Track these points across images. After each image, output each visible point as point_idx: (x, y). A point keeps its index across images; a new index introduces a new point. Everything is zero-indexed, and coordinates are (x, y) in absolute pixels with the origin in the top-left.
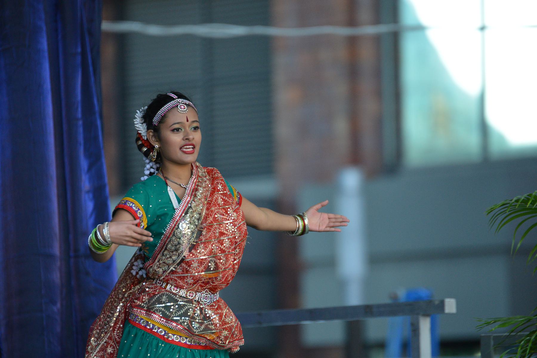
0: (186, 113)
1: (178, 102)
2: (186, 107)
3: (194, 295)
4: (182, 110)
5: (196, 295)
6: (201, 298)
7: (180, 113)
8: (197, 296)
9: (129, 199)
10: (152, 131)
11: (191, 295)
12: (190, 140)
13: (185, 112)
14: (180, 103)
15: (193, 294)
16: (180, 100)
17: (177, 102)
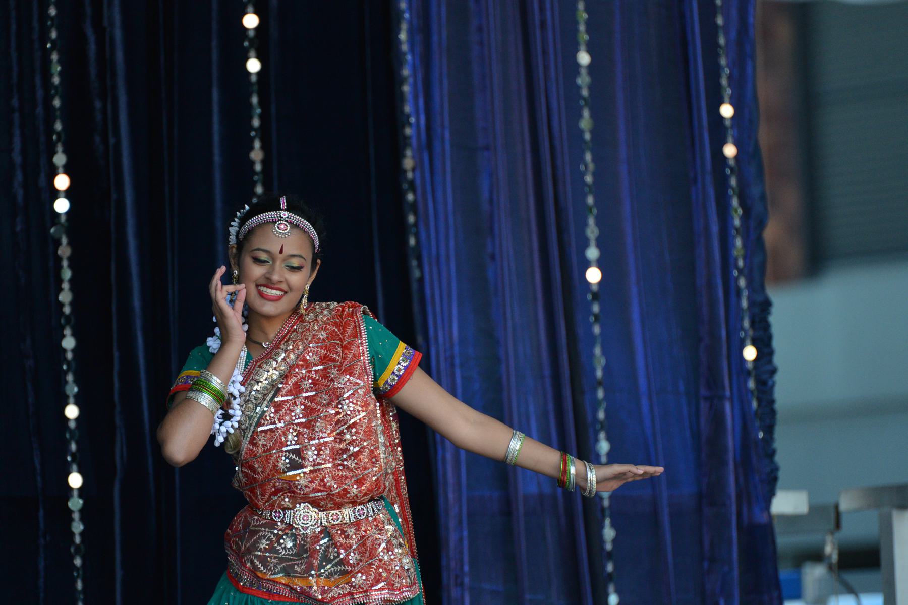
2: (289, 228)
5: (284, 515)
6: (293, 519)
9: (191, 373)
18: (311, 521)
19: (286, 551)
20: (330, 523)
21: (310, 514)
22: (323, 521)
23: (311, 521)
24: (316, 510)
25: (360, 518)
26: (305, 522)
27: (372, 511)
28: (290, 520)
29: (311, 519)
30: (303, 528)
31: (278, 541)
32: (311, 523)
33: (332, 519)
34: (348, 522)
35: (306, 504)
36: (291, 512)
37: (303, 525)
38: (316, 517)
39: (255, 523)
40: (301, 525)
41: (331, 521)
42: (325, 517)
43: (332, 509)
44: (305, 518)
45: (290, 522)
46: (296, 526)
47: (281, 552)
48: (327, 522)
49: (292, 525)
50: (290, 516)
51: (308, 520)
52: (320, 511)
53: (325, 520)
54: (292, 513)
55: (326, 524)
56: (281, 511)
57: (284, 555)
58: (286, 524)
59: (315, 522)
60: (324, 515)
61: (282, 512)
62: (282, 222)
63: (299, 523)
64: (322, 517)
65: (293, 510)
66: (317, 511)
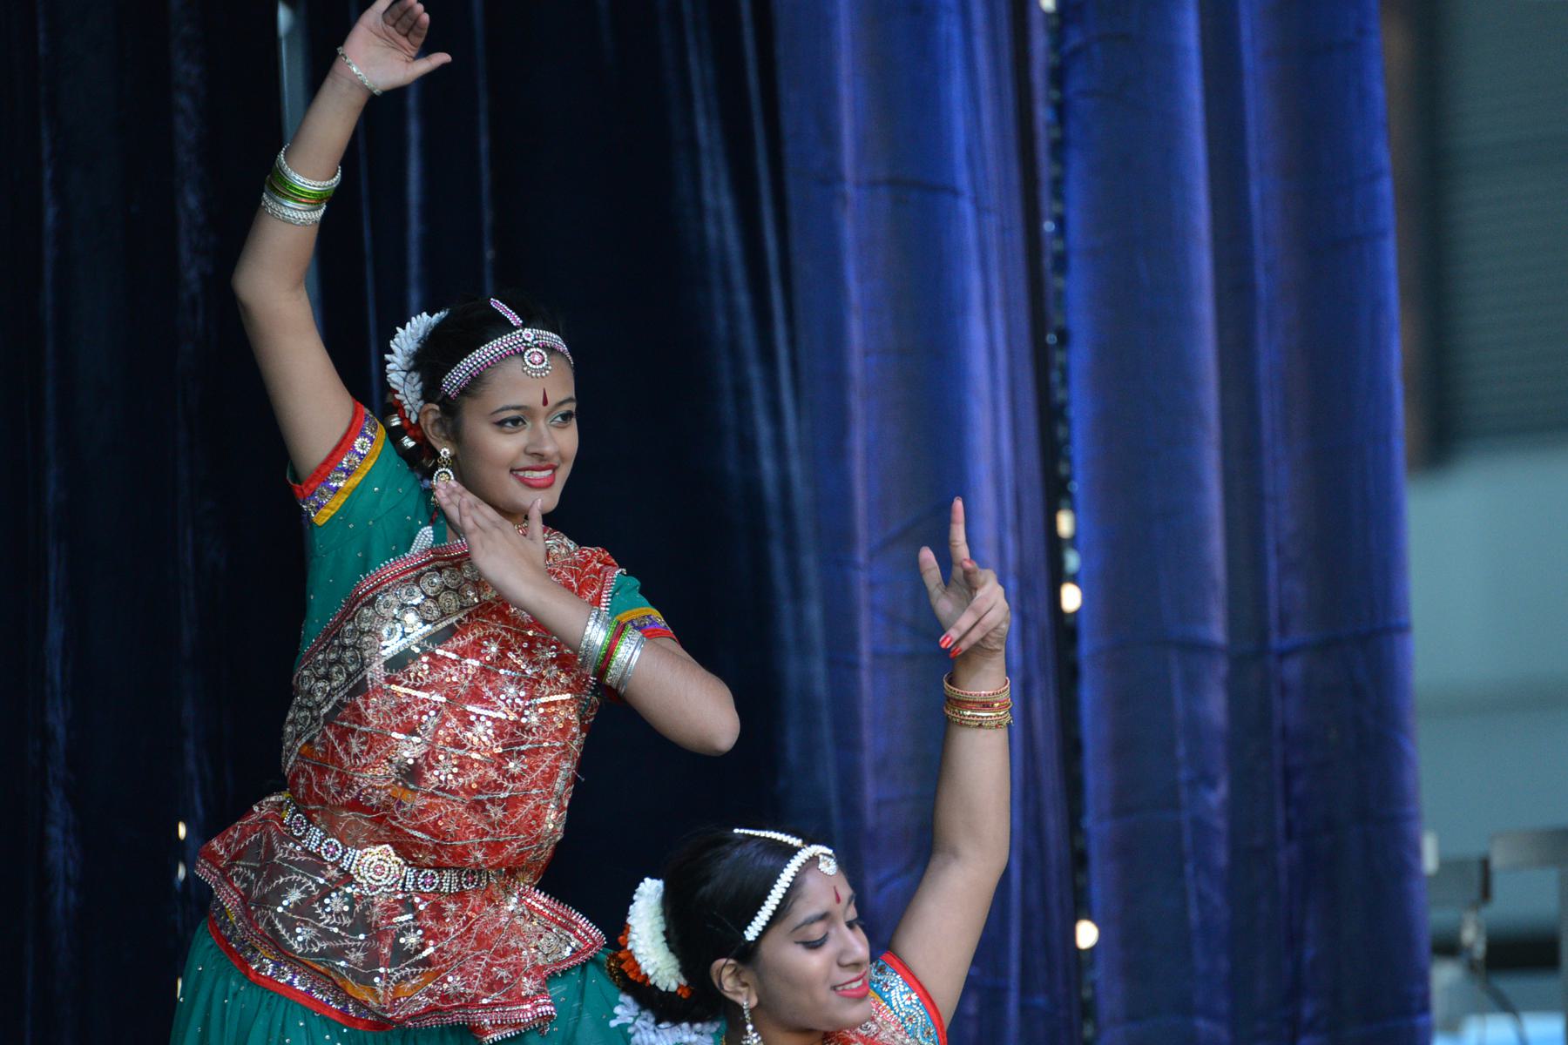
0: (541, 376)
1: (525, 341)
3: (339, 854)
4: (534, 367)
5: (343, 854)
7: (532, 377)
8: (348, 858)
10: (437, 408)
11: (429, 880)
12: (545, 457)
13: (539, 375)
14: (529, 345)
15: (325, 850)
17: (521, 340)
18: (386, 878)
23: (386, 878)
24: (399, 860)
26: (377, 878)
28: (350, 865)
29: (388, 876)
31: (321, 900)
32: (387, 881)
33: (422, 883)
35: (387, 846)
37: (371, 881)
39: (286, 855)
40: (368, 879)
44: (378, 870)
45: (349, 869)
46: (358, 879)
47: (324, 920)
50: (353, 859)
52: (407, 864)
53: (411, 883)
54: (358, 855)
56: (339, 845)
57: (328, 924)
58: (341, 870)
59: (392, 882)
61: (340, 848)
62: (532, 350)
63: (365, 876)
64: (408, 877)
65: (361, 850)
66: (402, 863)
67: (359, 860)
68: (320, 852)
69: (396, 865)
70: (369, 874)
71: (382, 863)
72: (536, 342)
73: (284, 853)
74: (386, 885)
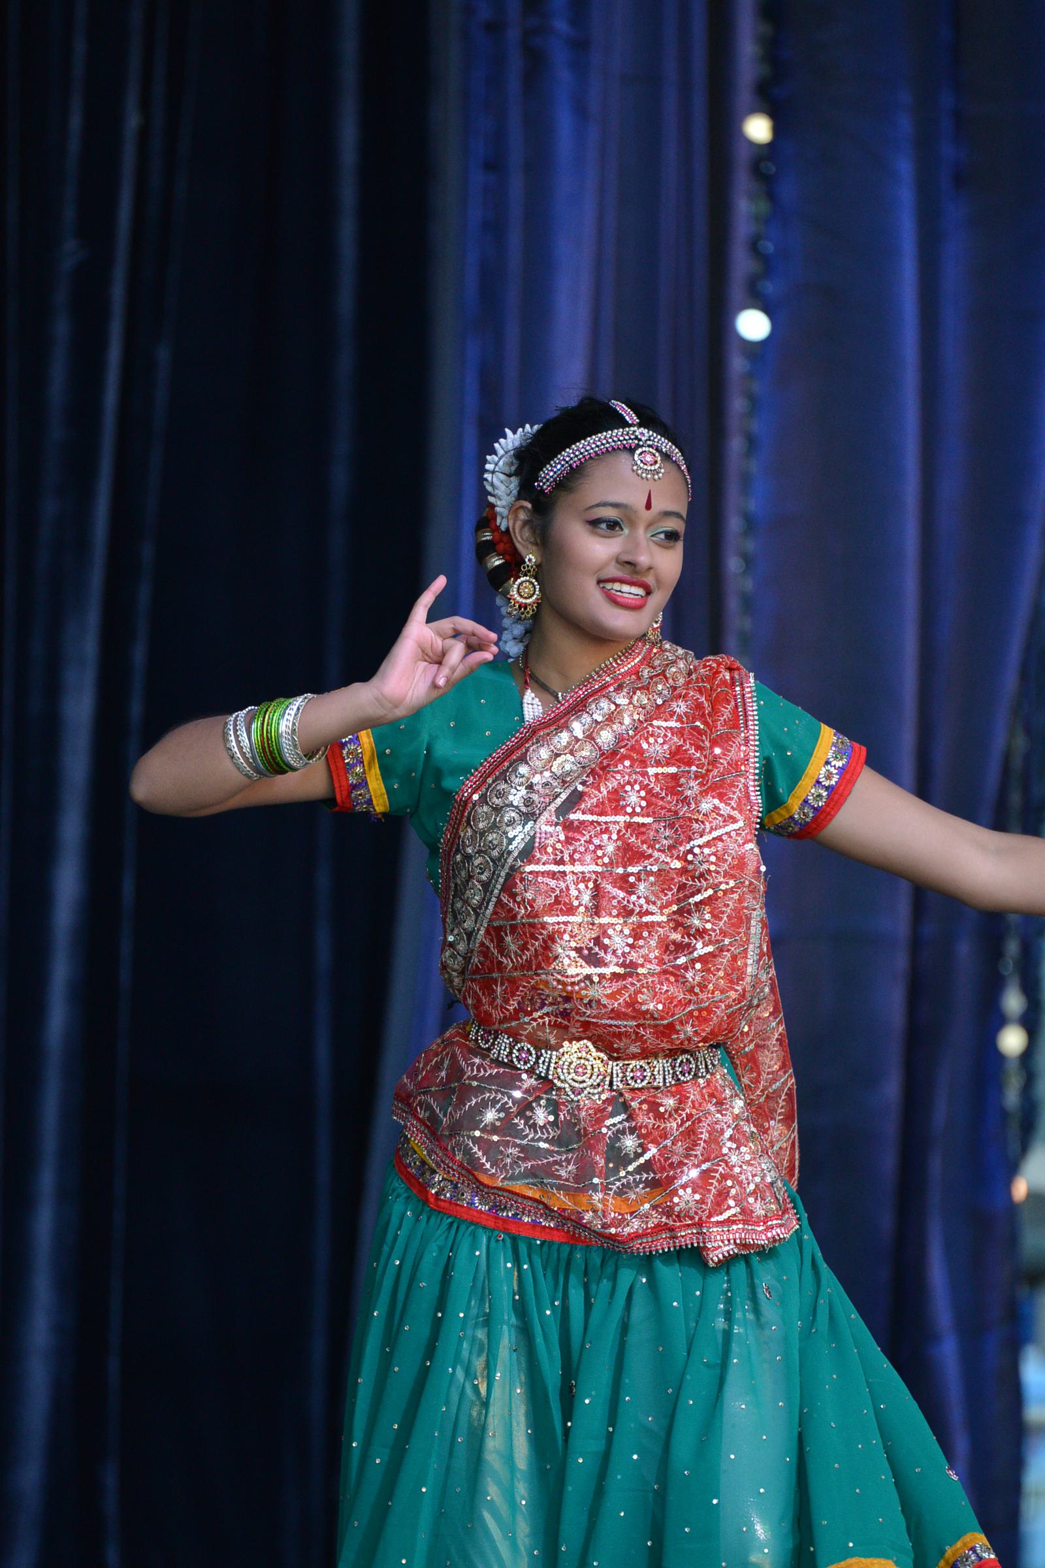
0: (659, 478)
1: (636, 438)
3: (533, 1059)
4: (645, 467)
5: (538, 1058)
8: (544, 1062)
14: (641, 443)
16: (645, 433)
18: (590, 1078)
19: (536, 1132)
20: (628, 1084)
21: (591, 1063)
22: (615, 1079)
23: (590, 1078)
24: (602, 1055)
25: (682, 1078)
26: (580, 1079)
27: (704, 1066)
28: (548, 1069)
30: (573, 1089)
32: (591, 1080)
33: (632, 1078)
34: (661, 1084)
35: (585, 1041)
36: (551, 1055)
38: (602, 1070)
39: (475, 1073)
40: (570, 1081)
41: (630, 1082)
42: (619, 1071)
43: (634, 1057)
44: (580, 1070)
45: (547, 1073)
48: (622, 1081)
49: (551, 1082)
50: (550, 1062)
51: (584, 1074)
52: (611, 1058)
53: (619, 1079)
54: (554, 1057)
55: (621, 1086)
56: (532, 1049)
58: (539, 1077)
59: (598, 1081)
60: (618, 1068)
61: (534, 1052)
62: (644, 449)
63: (566, 1079)
64: (615, 1072)
65: (557, 1051)
66: (605, 1058)
67: (556, 1063)
68: (512, 1061)
69: (599, 1062)
70: (570, 1077)
71: (582, 1061)
72: (648, 442)
73: (472, 1070)
74: (592, 1085)
